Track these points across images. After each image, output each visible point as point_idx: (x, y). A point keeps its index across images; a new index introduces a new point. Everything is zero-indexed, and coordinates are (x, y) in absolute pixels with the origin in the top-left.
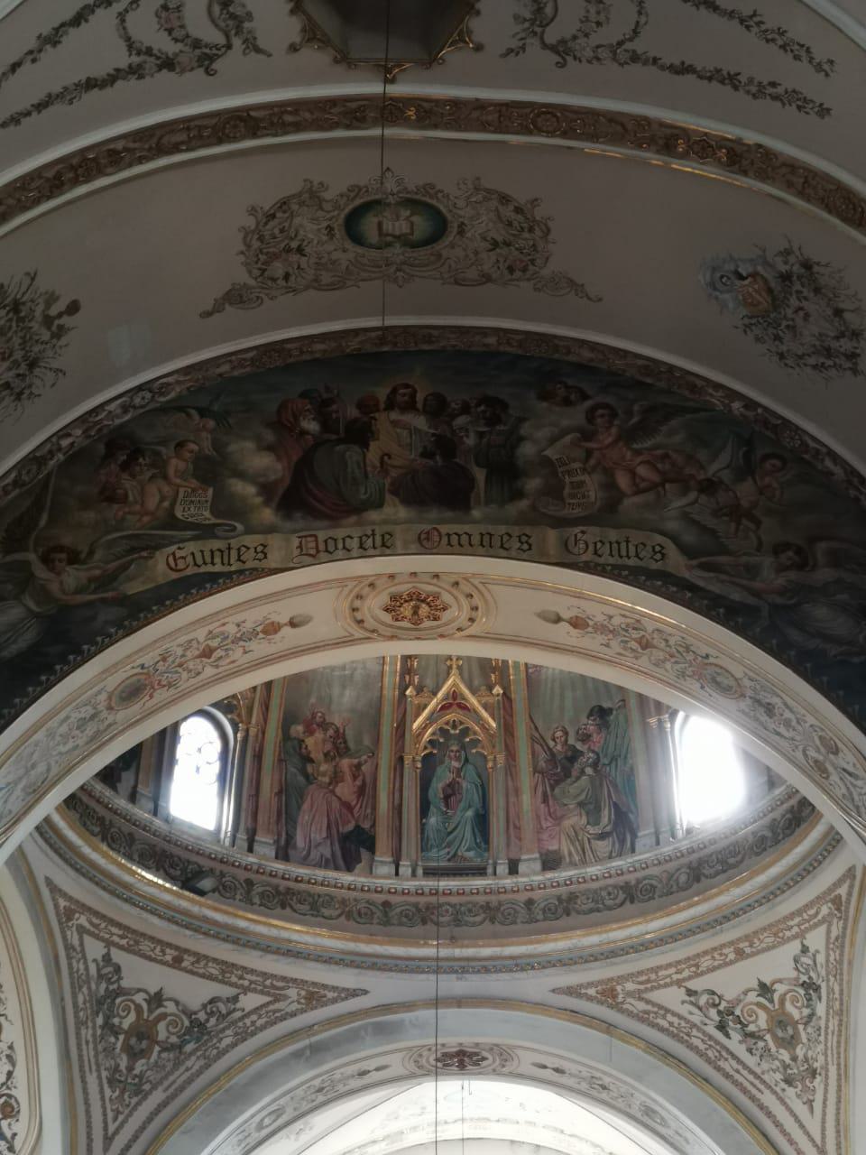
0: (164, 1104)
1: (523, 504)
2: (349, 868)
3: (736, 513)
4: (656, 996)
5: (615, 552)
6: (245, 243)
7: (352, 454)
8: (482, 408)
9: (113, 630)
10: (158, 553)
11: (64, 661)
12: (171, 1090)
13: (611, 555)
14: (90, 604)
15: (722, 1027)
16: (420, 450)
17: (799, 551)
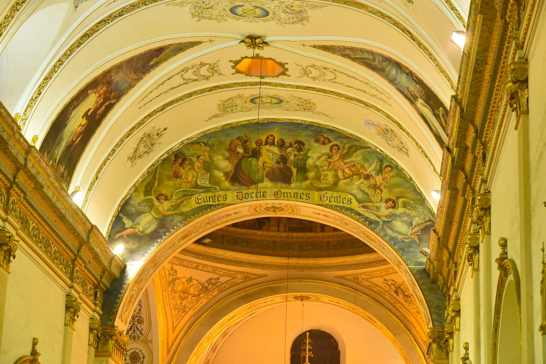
0: (194, 315)
1: (308, 182)
2: (260, 229)
3: (375, 187)
4: (373, 280)
5: (336, 201)
6: (218, 106)
7: (254, 161)
8: (296, 145)
9: (179, 224)
10: (192, 197)
11: (166, 235)
12: (196, 310)
13: (335, 202)
14: (172, 215)
15: (396, 292)
16: (276, 161)
17: (393, 202)
